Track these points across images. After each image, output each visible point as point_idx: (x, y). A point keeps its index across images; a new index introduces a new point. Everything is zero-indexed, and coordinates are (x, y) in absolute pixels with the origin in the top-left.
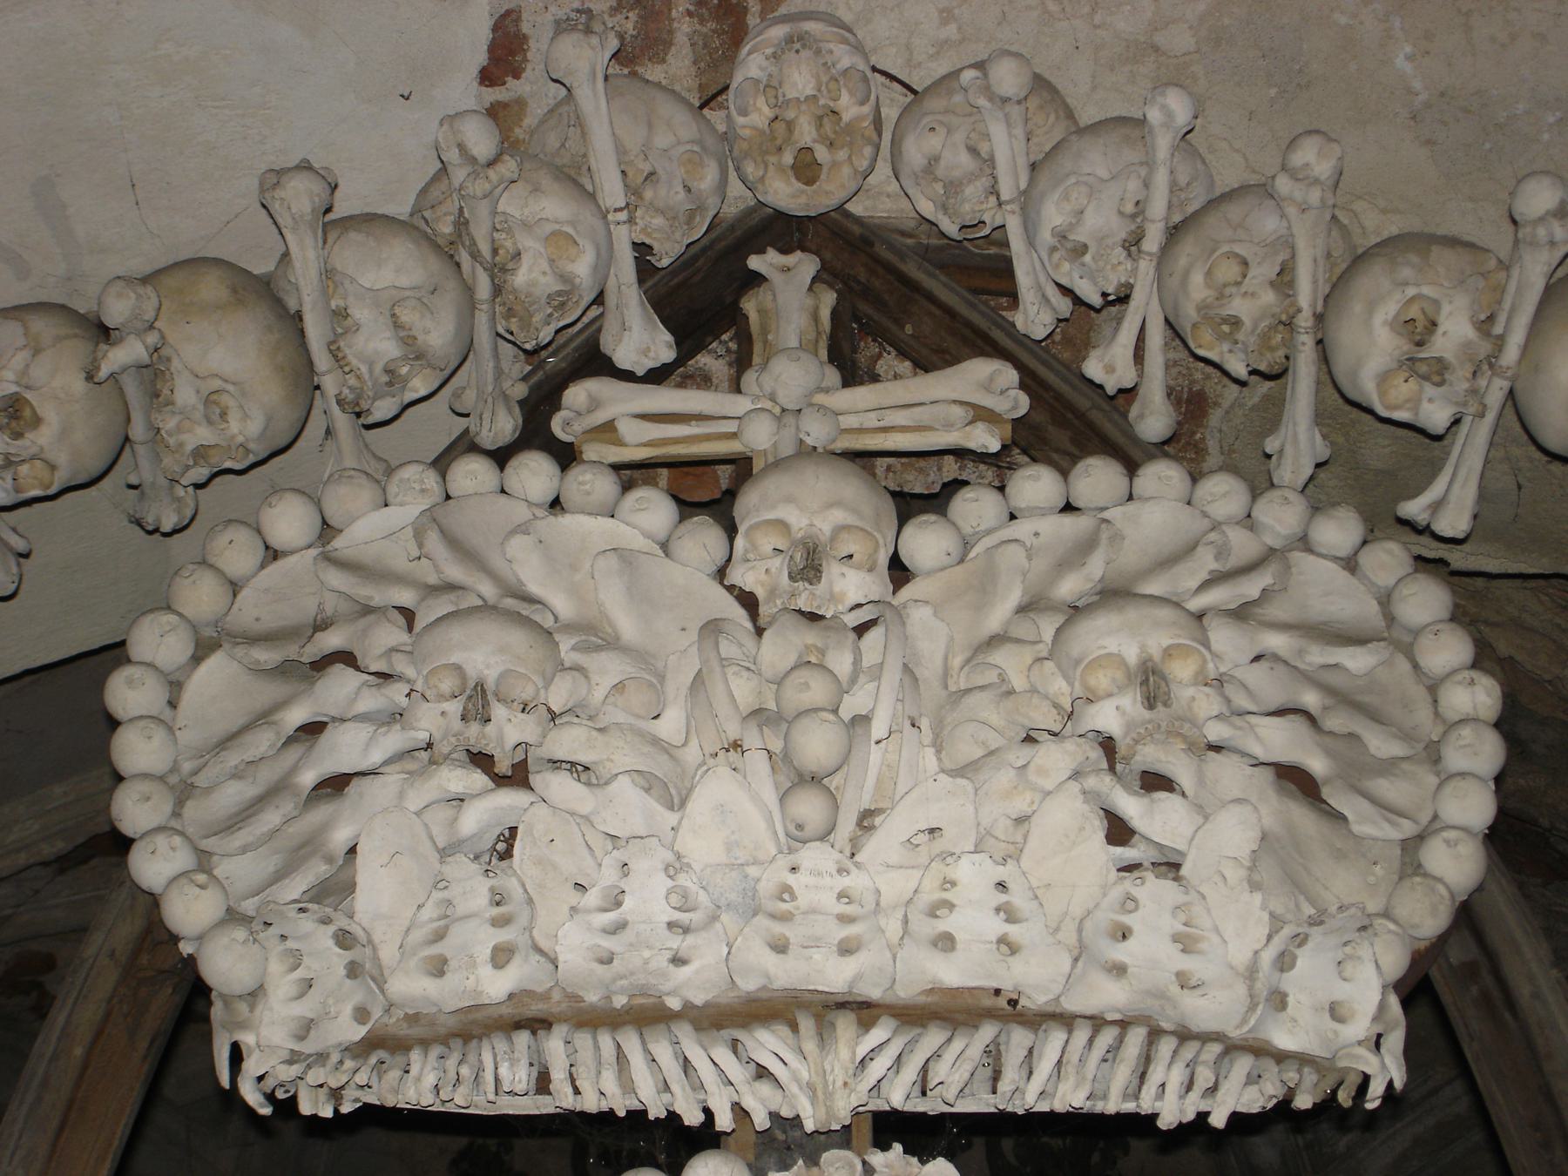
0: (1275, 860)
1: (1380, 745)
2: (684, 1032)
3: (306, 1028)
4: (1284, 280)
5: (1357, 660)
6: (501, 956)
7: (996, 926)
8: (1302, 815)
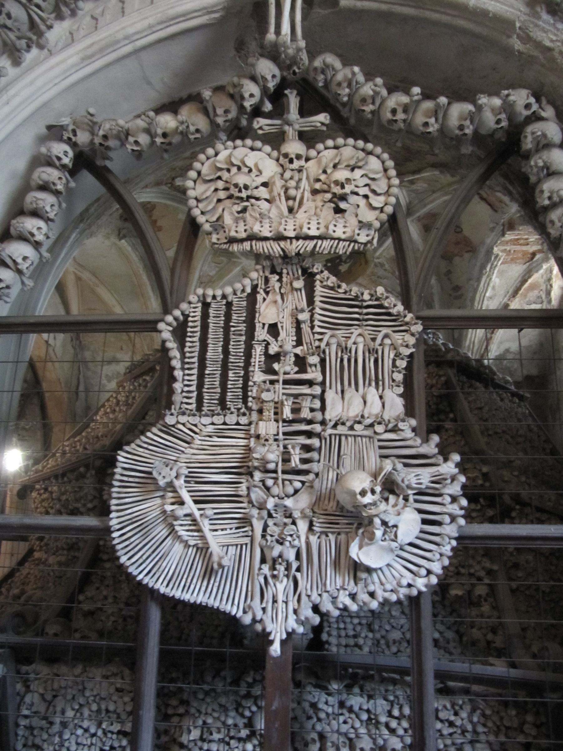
2: (272, 242)
3: (218, 239)
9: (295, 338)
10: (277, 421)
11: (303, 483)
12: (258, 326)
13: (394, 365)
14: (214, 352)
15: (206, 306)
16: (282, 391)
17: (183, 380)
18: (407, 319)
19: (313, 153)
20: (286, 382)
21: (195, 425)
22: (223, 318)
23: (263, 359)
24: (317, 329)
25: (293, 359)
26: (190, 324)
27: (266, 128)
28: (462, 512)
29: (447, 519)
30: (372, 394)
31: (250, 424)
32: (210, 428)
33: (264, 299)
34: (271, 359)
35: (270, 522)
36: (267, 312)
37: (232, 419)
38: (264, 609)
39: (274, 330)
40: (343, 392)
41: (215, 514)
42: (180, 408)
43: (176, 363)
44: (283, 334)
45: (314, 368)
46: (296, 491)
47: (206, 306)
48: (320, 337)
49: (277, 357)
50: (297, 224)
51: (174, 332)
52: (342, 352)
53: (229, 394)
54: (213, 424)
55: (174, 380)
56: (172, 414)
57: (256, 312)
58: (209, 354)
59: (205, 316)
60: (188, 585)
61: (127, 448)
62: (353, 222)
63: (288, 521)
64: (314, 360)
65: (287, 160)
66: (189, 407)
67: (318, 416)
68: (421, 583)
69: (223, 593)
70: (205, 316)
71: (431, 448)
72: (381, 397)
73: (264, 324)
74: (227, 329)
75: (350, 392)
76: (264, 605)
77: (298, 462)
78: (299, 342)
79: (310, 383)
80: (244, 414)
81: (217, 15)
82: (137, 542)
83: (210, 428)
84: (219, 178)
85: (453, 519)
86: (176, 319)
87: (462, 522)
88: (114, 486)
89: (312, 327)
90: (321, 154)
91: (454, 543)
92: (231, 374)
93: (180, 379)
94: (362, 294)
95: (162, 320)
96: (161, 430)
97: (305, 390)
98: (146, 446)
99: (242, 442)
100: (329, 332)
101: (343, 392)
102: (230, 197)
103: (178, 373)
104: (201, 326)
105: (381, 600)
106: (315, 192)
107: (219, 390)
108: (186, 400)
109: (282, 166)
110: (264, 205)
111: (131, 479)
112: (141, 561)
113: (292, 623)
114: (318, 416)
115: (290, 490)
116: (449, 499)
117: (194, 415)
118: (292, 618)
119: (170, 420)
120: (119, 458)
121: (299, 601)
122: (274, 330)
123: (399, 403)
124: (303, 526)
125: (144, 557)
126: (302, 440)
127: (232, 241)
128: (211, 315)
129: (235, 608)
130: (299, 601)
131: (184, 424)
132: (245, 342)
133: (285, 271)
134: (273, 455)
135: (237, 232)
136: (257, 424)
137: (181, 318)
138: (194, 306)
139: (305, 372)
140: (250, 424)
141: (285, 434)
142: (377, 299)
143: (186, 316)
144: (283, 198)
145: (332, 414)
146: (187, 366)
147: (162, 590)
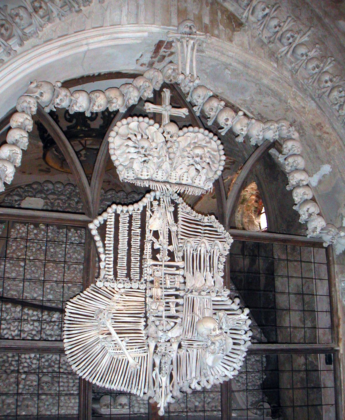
0: (207, 174)
1: (216, 162)
3: (128, 177)
4: (216, 112)
5: (215, 153)
6: (147, 175)
7: (186, 178)
8: (208, 166)
9: (168, 240)
10: (162, 288)
11: (176, 323)
12: (147, 230)
13: (219, 260)
14: (123, 245)
15: (117, 216)
16: (163, 272)
17: (105, 260)
18: (226, 236)
19: (181, 133)
20: (165, 266)
21: (114, 288)
22: (128, 225)
23: (151, 251)
24: (180, 237)
25: (167, 252)
26: (108, 226)
27: (151, 109)
28: (250, 338)
29: (242, 342)
30: (209, 275)
31: (146, 289)
32: (123, 290)
33: (151, 216)
34: (155, 252)
35: (159, 345)
36: (155, 223)
37: (135, 286)
38: (155, 391)
39: (156, 234)
40: (193, 273)
41: (130, 340)
42: (104, 278)
43: (101, 250)
44: (161, 237)
45: (178, 259)
46: (172, 328)
47: (117, 216)
48: (182, 241)
49: (158, 251)
50: (177, 176)
51: (98, 229)
52: (193, 250)
53: (132, 270)
54: (124, 288)
55: (100, 260)
56: (100, 281)
57: (145, 223)
58: (120, 246)
59: (117, 222)
60: (112, 380)
61: (71, 300)
62: (204, 178)
63: (169, 344)
64: (181, 254)
65: (169, 135)
66: (110, 277)
67: (182, 287)
68: (230, 375)
69: (132, 383)
70: (117, 222)
71: (235, 307)
72: (213, 277)
73: (151, 230)
74: (130, 230)
75: (197, 274)
76: (155, 389)
77: (175, 312)
78: (170, 243)
79: (178, 268)
80: (142, 283)
81: (139, 42)
82: (82, 356)
83: (123, 290)
84: (129, 139)
85: (245, 342)
86: (100, 223)
87: (250, 343)
88: (65, 324)
89: (177, 235)
90: (186, 135)
91: (245, 354)
92: (132, 258)
93: (103, 260)
94: (204, 219)
95: (91, 222)
96: (92, 290)
97: (173, 271)
98: (84, 299)
99: (143, 299)
100: (189, 239)
101: (193, 273)
102: (139, 152)
103: (102, 257)
104: (115, 228)
105: (212, 383)
106: (183, 157)
107: (126, 268)
108: (108, 273)
109: (165, 138)
110: (156, 160)
111: (76, 319)
112: (84, 367)
113: (169, 399)
114: (182, 287)
115: (169, 327)
116: (244, 332)
117: (113, 282)
118: (169, 396)
119: (99, 284)
120: (67, 306)
121: (173, 386)
122: (156, 234)
123: (222, 280)
124: (175, 346)
125: (86, 365)
126: (173, 299)
127: (138, 179)
128: (120, 222)
129: (139, 391)
130: (173, 386)
131: (106, 287)
132: (141, 241)
133: (162, 200)
134: (162, 308)
135: (142, 175)
136: (150, 289)
137: (102, 223)
138: (109, 215)
139: (174, 261)
140: (146, 289)
141: (165, 295)
142: (211, 223)
143: (105, 221)
144: (168, 158)
145: (189, 285)
146: (107, 252)
147: (98, 383)
